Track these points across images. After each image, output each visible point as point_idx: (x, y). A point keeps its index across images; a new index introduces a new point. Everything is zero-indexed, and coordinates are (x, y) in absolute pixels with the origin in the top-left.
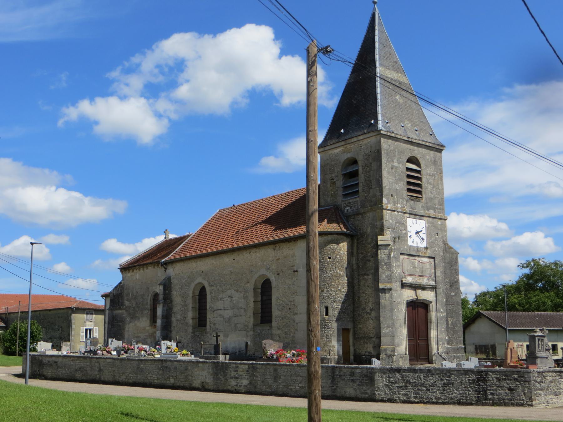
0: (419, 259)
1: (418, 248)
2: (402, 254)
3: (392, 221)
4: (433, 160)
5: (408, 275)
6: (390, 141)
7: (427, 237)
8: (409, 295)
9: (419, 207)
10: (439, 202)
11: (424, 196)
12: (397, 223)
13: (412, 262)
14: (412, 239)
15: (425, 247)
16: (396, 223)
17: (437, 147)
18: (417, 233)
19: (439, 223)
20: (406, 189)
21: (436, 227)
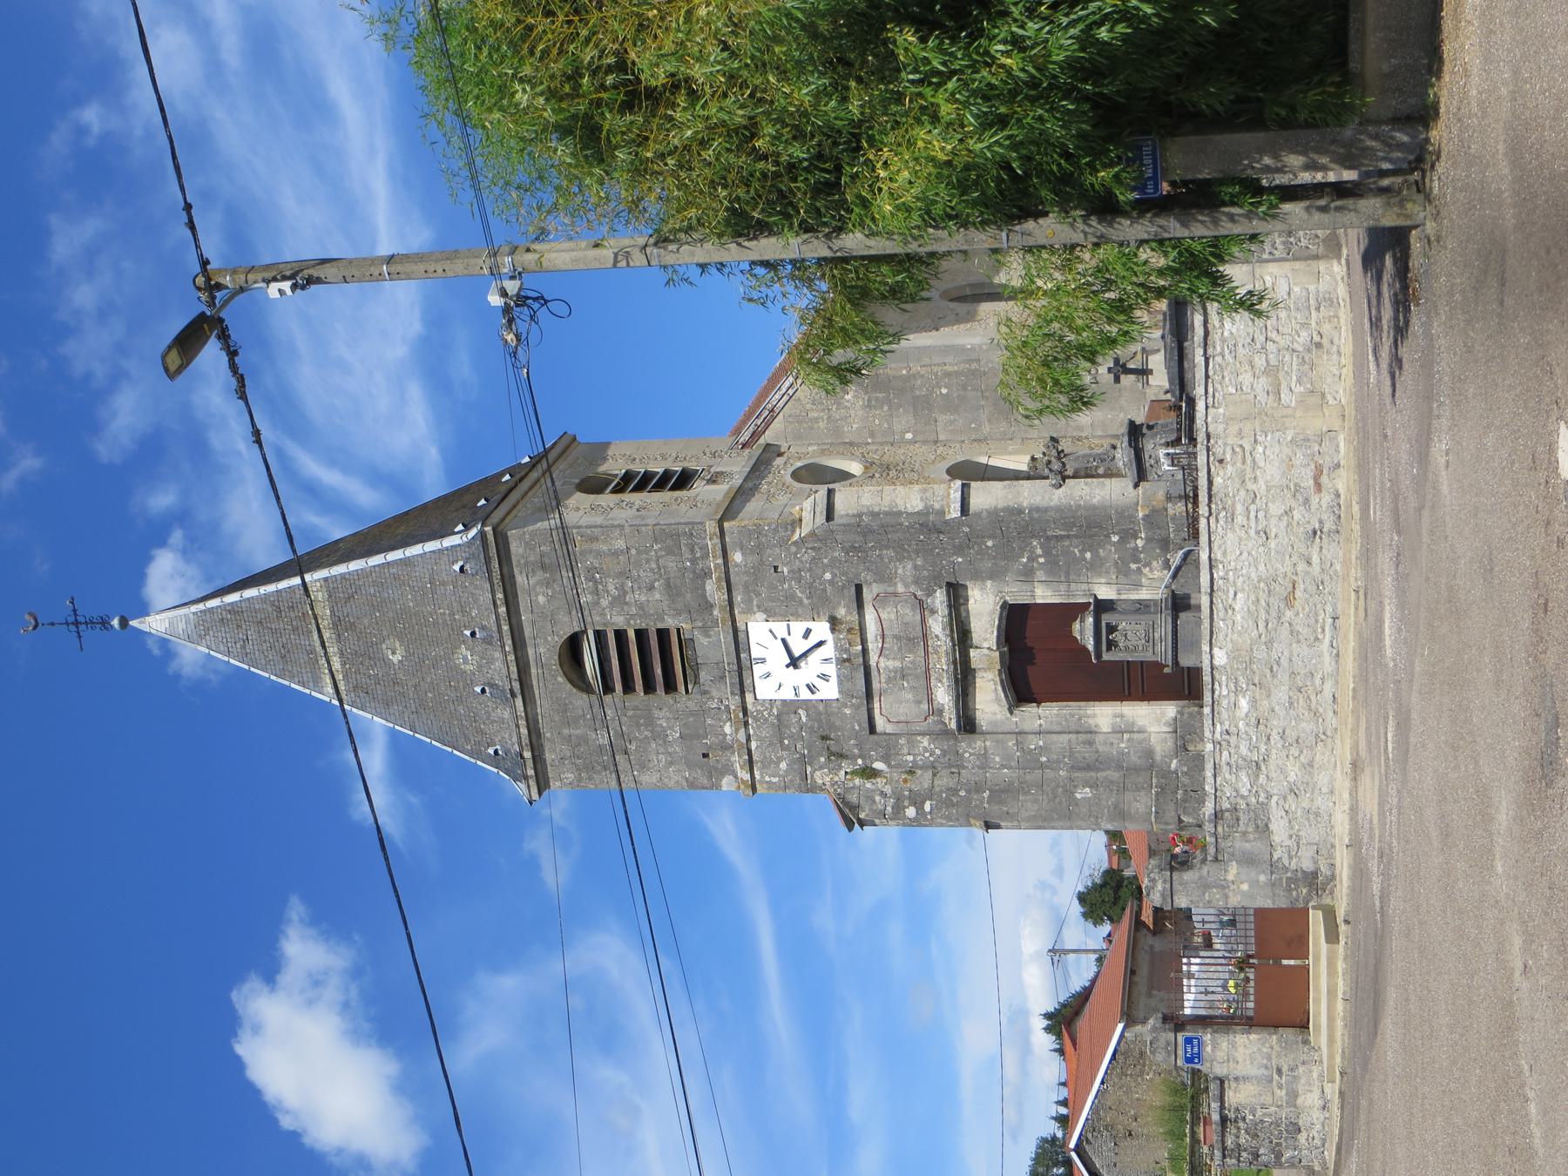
0: (873, 647)
1: (841, 662)
2: (872, 728)
3: (780, 760)
4: (540, 575)
5: (930, 700)
6: (549, 756)
7: (798, 617)
8: (989, 698)
9: (711, 646)
10: (670, 552)
11: (670, 623)
12: (781, 742)
13: (889, 680)
14: (819, 683)
15: (833, 630)
16: (784, 748)
17: (495, 564)
18: (794, 662)
19: (737, 557)
20: (669, 699)
21: (756, 573)
